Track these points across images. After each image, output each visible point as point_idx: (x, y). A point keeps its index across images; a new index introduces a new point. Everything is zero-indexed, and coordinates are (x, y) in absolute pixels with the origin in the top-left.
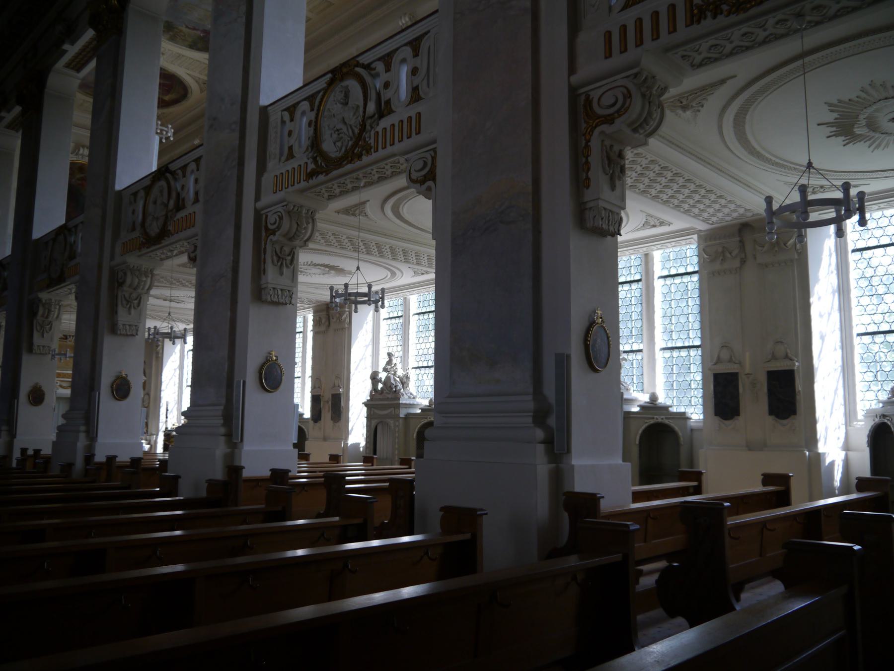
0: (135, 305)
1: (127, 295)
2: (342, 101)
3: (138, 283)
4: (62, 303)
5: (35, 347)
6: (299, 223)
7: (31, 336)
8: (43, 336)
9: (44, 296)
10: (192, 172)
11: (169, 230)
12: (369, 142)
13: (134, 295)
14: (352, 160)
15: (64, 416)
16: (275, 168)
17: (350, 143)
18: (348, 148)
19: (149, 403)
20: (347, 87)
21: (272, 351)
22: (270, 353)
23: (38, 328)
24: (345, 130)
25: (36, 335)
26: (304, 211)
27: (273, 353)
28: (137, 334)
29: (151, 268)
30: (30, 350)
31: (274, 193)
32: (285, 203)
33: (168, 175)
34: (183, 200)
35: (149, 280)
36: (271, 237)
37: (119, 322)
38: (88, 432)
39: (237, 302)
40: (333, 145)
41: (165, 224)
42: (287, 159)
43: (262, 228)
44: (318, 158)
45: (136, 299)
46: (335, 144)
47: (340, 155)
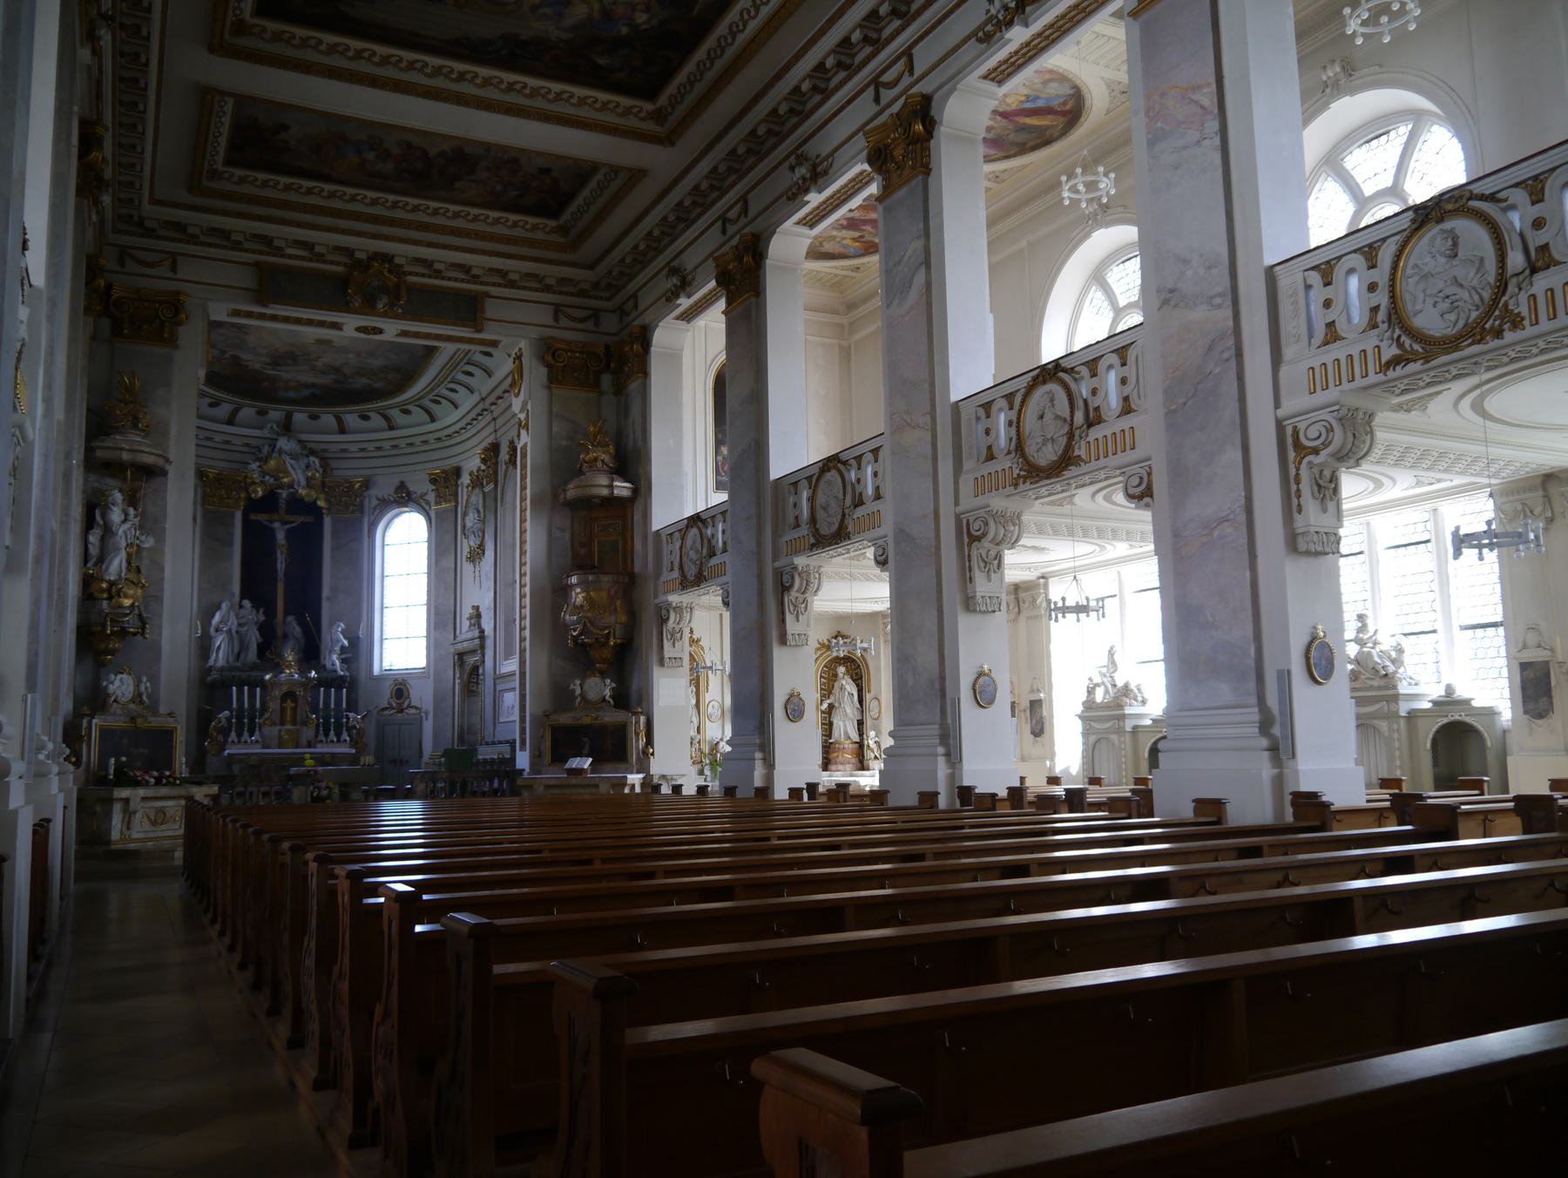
0: (996, 569)
1: (984, 555)
2: (1448, 252)
3: (1004, 535)
4: (822, 569)
5: (789, 637)
6: (1357, 435)
7: (783, 621)
8: (798, 621)
9: (800, 561)
10: (1110, 367)
11: (1079, 456)
12: (1516, 311)
13: (993, 553)
14: (1482, 339)
15: (891, 734)
16: (1301, 357)
17: (1474, 314)
18: (1470, 320)
19: (880, 712)
20: (1452, 230)
21: (1317, 624)
22: (1315, 628)
23: (792, 609)
24: (1465, 295)
25: (789, 618)
26: (1361, 415)
27: (1320, 627)
28: (1000, 610)
29: (1019, 511)
30: (783, 640)
31: (1311, 393)
32: (1337, 407)
33: (1061, 374)
34: (1097, 409)
35: (1017, 527)
36: (1310, 458)
37: (977, 594)
38: (948, 755)
39: (1256, 557)
40: (1440, 317)
41: (1069, 447)
42: (1326, 343)
43: (1291, 445)
44: (1403, 338)
45: (995, 559)
46: (1442, 316)
47: (1454, 332)
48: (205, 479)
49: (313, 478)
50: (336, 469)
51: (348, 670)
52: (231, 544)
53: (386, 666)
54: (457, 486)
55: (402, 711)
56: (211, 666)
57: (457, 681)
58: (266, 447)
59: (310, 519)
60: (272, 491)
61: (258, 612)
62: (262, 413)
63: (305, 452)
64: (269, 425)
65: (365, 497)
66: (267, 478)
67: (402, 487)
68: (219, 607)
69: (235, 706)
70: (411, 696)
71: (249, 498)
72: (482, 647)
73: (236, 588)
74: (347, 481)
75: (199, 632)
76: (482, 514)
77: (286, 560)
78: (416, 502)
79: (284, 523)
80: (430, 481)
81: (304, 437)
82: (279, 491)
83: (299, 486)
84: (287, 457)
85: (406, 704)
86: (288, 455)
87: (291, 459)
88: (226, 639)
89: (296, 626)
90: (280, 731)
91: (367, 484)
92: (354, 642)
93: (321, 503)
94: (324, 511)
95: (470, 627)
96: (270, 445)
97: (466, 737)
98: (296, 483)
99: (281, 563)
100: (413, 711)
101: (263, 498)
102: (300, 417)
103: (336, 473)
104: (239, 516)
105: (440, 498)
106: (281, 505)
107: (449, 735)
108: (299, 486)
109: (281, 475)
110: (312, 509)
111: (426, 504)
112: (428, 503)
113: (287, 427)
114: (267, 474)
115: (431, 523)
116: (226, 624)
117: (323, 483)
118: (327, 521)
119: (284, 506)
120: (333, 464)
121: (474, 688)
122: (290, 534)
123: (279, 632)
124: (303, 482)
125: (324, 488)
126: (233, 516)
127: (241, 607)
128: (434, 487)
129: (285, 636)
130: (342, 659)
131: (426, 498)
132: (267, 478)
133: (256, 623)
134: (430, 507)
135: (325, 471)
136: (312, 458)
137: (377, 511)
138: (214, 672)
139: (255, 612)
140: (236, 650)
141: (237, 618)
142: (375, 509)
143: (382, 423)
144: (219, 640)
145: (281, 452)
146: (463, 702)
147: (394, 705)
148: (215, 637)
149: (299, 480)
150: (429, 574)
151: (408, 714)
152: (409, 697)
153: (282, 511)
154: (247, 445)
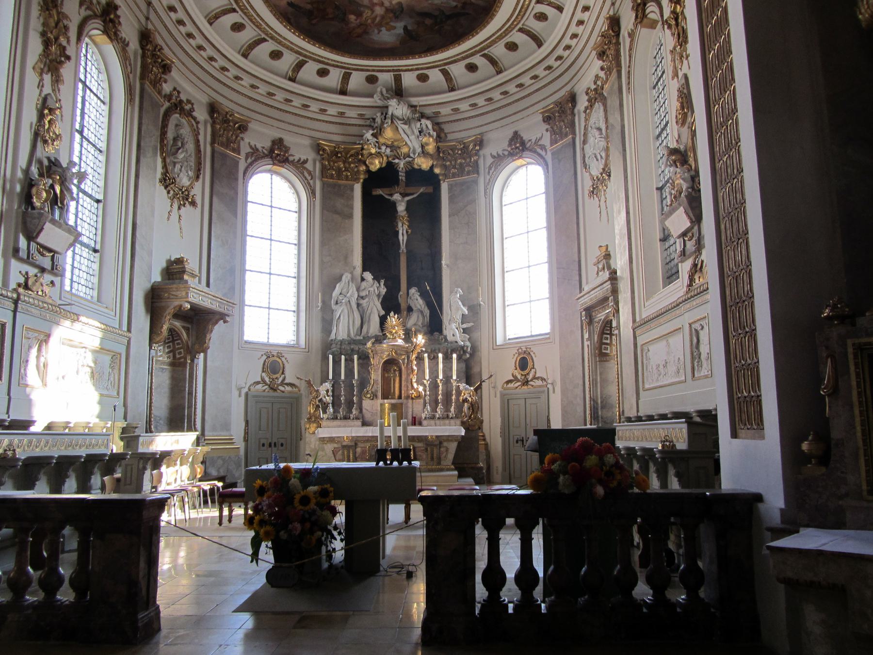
48: (321, 153)
49: (427, 144)
50: (450, 133)
51: (469, 340)
52: (350, 216)
53: (511, 334)
54: (573, 114)
55: (526, 383)
56: (332, 340)
57: (586, 343)
58: (379, 114)
59: (430, 190)
60: (389, 164)
61: (379, 283)
62: (372, 80)
63: (417, 115)
64: (379, 89)
65: (479, 157)
66: (384, 148)
67: (516, 135)
68: (339, 279)
69: (331, 377)
70: (535, 367)
71: (368, 171)
72: (615, 291)
73: (357, 259)
74: (460, 142)
75: (320, 304)
76: (604, 131)
77: (407, 232)
78: (531, 150)
79: (404, 195)
80: (544, 121)
81: (414, 101)
82: (397, 161)
83: (414, 154)
84: (399, 122)
85: (530, 377)
86: (400, 120)
87: (405, 124)
88: (346, 311)
89: (419, 298)
90: (382, 405)
91: (480, 143)
92: (474, 309)
93: (437, 171)
94: (441, 178)
95: (598, 273)
96: (382, 114)
97: (600, 413)
98: (411, 150)
99: (403, 234)
100: (539, 383)
101: (380, 169)
102: (409, 80)
103: (450, 137)
104: (358, 189)
105: (557, 134)
106: (400, 178)
107: (580, 409)
108: (414, 154)
109: (396, 143)
110: (430, 179)
111: (541, 149)
112: (543, 147)
113: (398, 92)
114: (382, 145)
115: (547, 168)
116: (345, 296)
117: (438, 148)
118: (444, 187)
119: (404, 178)
120: (447, 128)
121: (608, 351)
122: (409, 206)
123: (403, 306)
124: (419, 150)
125: (439, 155)
126: (352, 190)
127: (363, 279)
128: (548, 127)
129: (410, 309)
130: (463, 329)
131: (540, 143)
132: (384, 148)
133: (379, 296)
134: (546, 151)
135: (438, 136)
136: (423, 121)
137: (493, 169)
138: (334, 346)
139: (376, 284)
140: (358, 322)
141: (358, 290)
142: (490, 168)
143: (491, 69)
144: (340, 311)
145: (393, 117)
146: (593, 372)
147: (519, 377)
148: (336, 310)
149: (414, 147)
150: (548, 228)
151: (532, 386)
152: (533, 368)
153: (402, 184)
154: (361, 116)
